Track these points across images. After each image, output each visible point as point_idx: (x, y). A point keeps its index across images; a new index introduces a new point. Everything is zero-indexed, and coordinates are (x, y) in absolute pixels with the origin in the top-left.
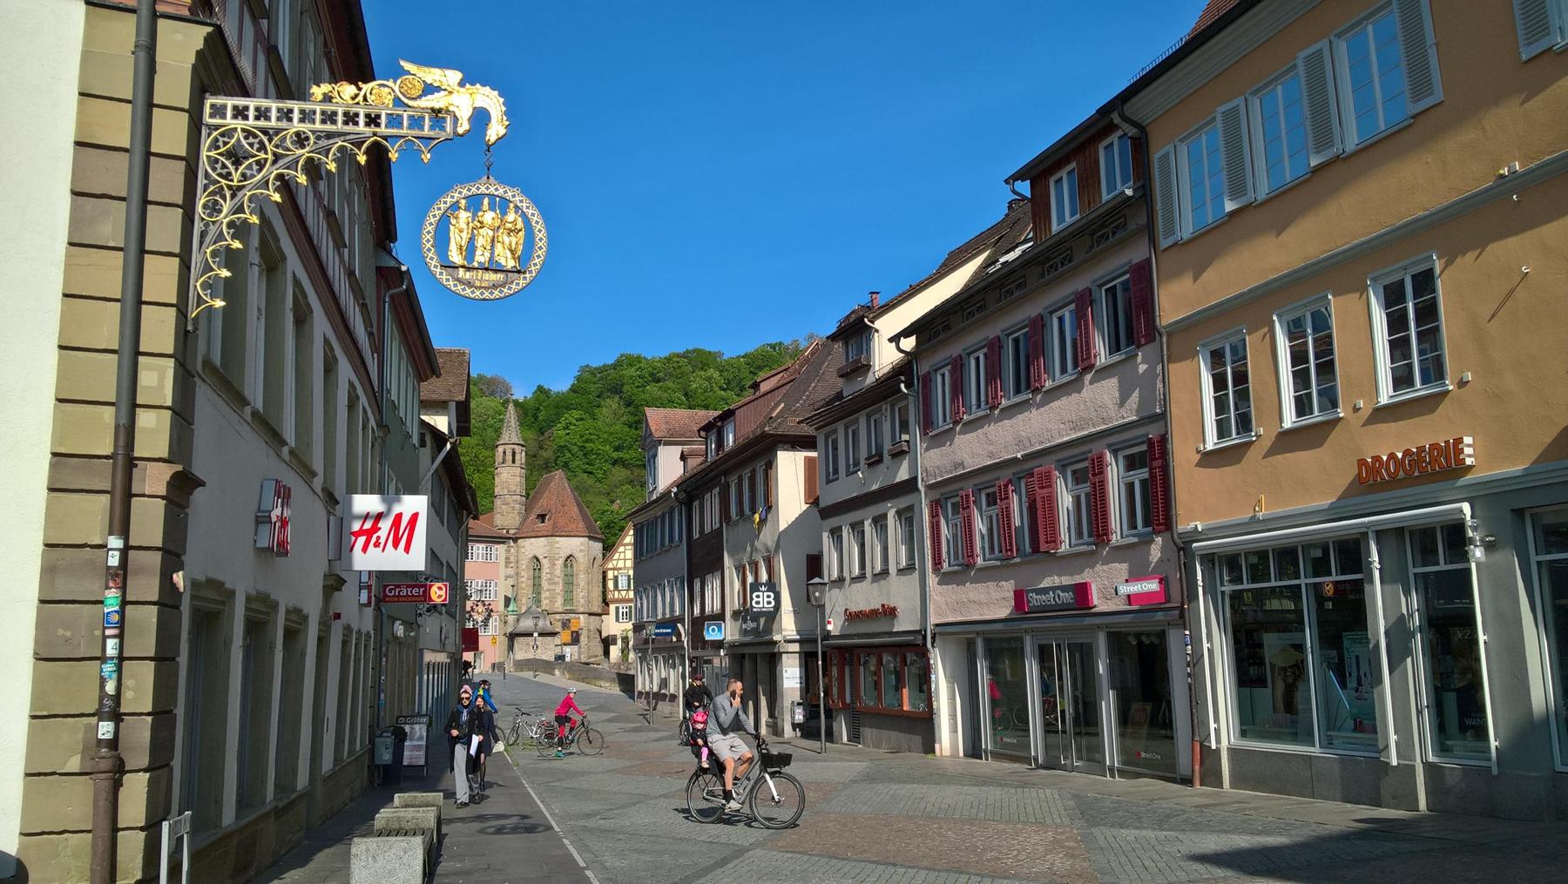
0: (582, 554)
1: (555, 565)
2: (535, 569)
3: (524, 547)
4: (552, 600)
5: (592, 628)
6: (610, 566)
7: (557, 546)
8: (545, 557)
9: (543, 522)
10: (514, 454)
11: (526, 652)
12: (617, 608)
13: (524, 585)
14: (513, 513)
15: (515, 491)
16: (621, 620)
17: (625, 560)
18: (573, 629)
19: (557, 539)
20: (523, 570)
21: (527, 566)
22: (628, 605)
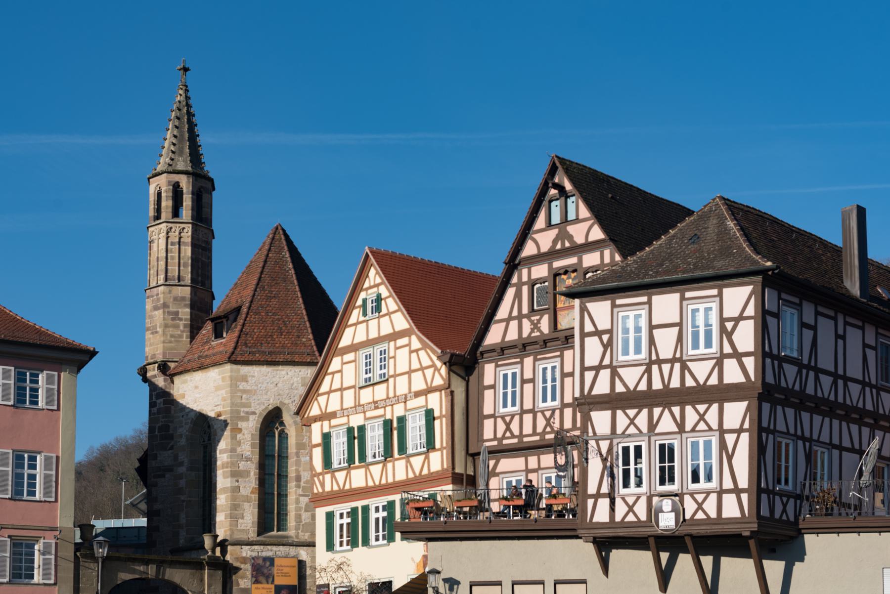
2: (205, 447)
7: (242, 386)
9: (221, 336)
13: (182, 483)
14: (177, 327)
18: (279, 581)
19: (245, 370)
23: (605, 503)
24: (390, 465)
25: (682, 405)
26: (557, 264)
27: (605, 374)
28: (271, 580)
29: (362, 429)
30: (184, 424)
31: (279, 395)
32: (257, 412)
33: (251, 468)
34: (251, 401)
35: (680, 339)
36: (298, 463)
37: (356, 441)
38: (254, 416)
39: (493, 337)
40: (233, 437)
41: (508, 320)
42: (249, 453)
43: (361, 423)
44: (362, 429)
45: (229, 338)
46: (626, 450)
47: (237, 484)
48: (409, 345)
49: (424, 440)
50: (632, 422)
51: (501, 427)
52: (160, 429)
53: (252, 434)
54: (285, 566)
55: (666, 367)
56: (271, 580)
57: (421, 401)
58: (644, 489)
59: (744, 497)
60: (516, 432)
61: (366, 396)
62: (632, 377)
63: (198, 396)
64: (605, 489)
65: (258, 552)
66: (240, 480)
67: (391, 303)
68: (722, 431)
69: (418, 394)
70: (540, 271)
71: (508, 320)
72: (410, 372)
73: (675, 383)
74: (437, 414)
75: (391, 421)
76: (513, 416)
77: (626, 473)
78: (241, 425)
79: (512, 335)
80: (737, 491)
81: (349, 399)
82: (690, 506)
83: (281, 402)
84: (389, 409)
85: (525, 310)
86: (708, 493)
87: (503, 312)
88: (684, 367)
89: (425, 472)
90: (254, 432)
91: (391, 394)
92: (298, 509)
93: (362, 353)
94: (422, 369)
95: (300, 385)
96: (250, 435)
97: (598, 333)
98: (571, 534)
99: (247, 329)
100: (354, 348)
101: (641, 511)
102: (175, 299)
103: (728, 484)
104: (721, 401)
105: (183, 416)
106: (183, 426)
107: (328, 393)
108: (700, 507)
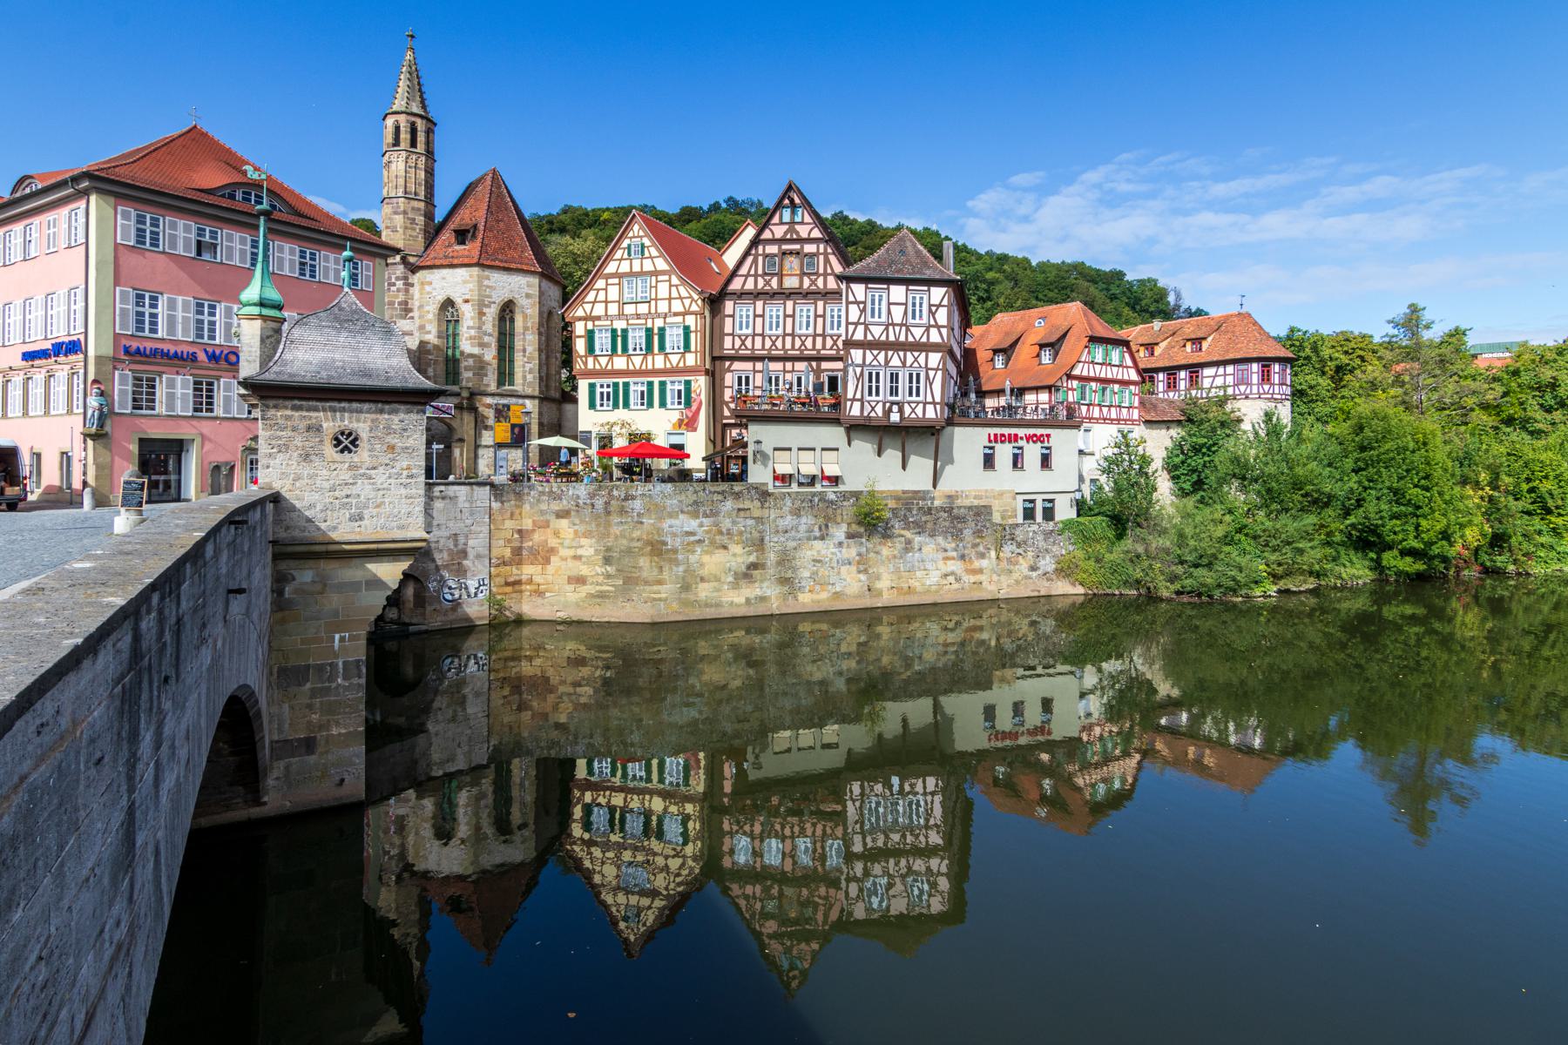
5: (545, 422)
6: (580, 313)
7: (486, 282)
8: (467, 301)
9: (462, 243)
10: (413, 131)
11: (306, 457)
12: (592, 387)
16: (598, 407)
17: (606, 302)
18: (514, 421)
19: (487, 273)
20: (430, 322)
22: (611, 381)
23: (857, 405)
24: (650, 358)
25: (905, 350)
26: (785, 247)
27: (861, 328)
29: (625, 331)
33: (492, 341)
35: (906, 313)
36: (524, 340)
37: (619, 339)
39: (736, 285)
40: (480, 319)
41: (747, 276)
43: (625, 326)
44: (625, 331)
45: (471, 249)
46: (870, 374)
48: (670, 281)
49: (682, 345)
50: (875, 358)
51: (738, 343)
52: (400, 303)
55: (897, 328)
57: (679, 319)
58: (881, 398)
59: (938, 407)
60: (750, 346)
61: (629, 309)
62: (877, 331)
64: (858, 396)
67: (654, 252)
68: (928, 369)
69: (676, 314)
70: (772, 249)
71: (747, 276)
72: (670, 299)
73: (902, 338)
74: (693, 328)
75: (652, 329)
76: (747, 336)
77: (870, 387)
78: (485, 310)
79: (750, 285)
80: (934, 403)
81: (613, 309)
82: (907, 410)
84: (650, 321)
85: (760, 272)
86: (918, 403)
87: (744, 270)
88: (908, 330)
89: (681, 365)
91: (653, 311)
92: (524, 372)
93: (625, 281)
94: (681, 298)
97: (857, 303)
98: (836, 422)
99: (486, 241)
100: (616, 275)
101: (879, 410)
103: (929, 399)
104: (927, 351)
107: (594, 303)
108: (913, 410)
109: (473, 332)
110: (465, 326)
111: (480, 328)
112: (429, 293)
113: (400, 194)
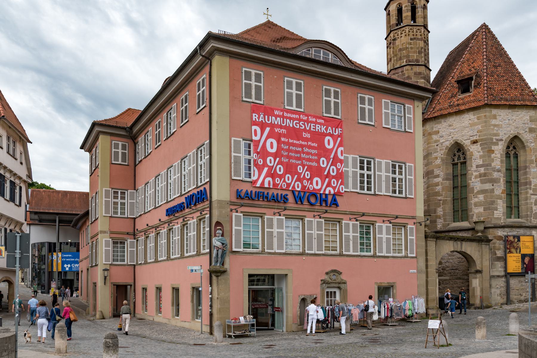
0: (533, 135)
1: (493, 152)
3: (437, 132)
4: (490, 206)
8: (475, 142)
15: (417, 61)
21: (442, 160)
28: (518, 251)
30: (439, 150)
31: (517, 128)
32: (504, 139)
34: (499, 132)
38: (502, 142)
42: (499, 167)
47: (493, 187)
53: (501, 154)
54: (527, 241)
56: (518, 251)
63: (452, 131)
65: (507, 232)
66: (494, 185)
83: (518, 133)
90: (502, 153)
95: (529, 121)
96: (499, 155)
102: (415, 73)
105: (437, 145)
106: (438, 152)
109: (482, 170)
110: (474, 166)
111: (490, 165)
112: (436, 141)
113: (405, 64)
